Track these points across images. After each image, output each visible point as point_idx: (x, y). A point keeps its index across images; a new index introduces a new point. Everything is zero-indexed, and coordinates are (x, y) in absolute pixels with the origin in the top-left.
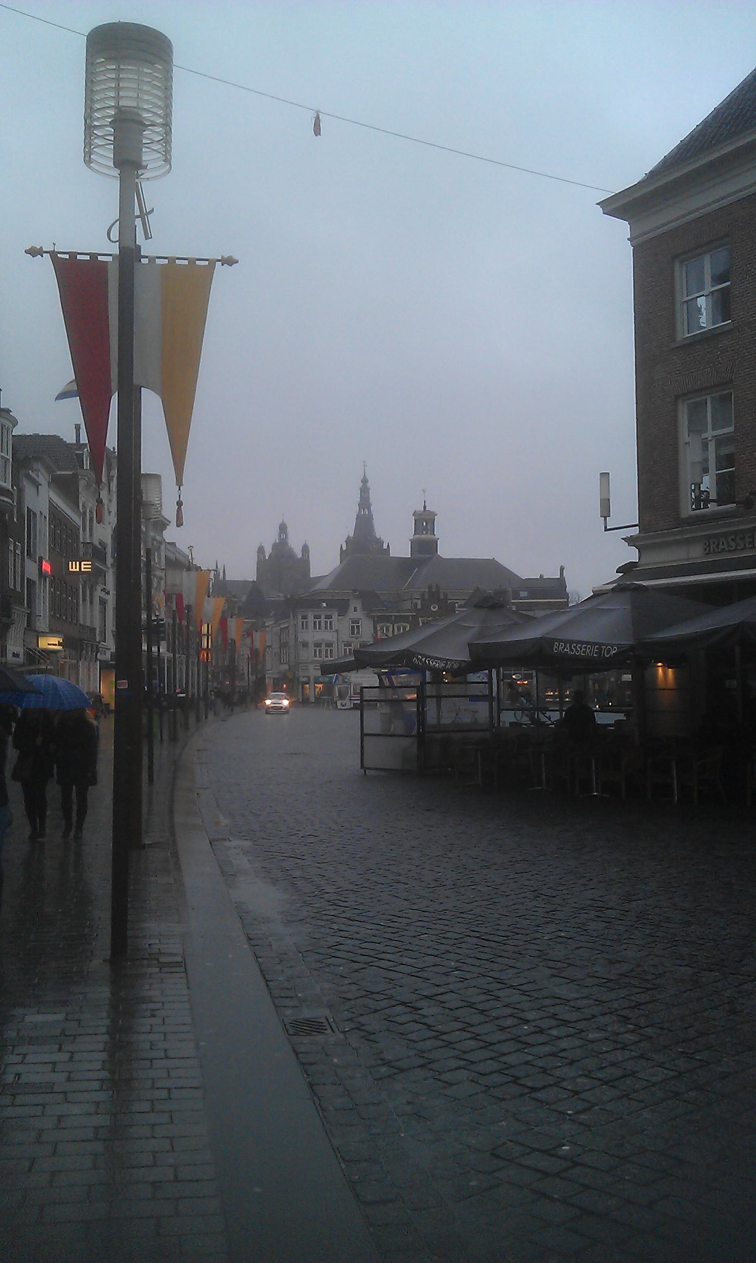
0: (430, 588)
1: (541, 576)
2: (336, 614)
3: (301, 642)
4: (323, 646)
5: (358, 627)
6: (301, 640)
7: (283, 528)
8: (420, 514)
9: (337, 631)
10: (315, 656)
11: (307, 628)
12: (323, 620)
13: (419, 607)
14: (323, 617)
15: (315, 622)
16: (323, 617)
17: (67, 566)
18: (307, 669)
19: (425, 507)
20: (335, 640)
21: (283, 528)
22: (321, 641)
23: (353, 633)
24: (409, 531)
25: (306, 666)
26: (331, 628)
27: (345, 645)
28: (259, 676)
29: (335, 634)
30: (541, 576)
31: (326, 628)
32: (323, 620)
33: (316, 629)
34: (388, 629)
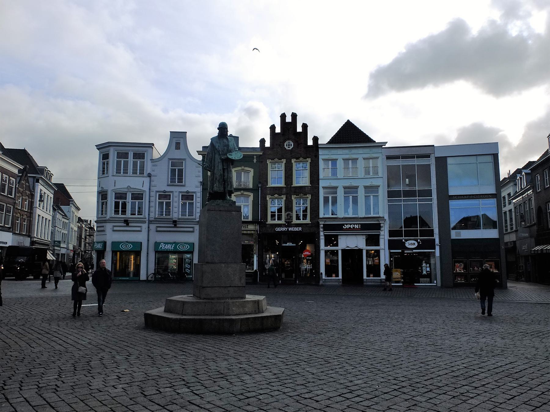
4: (129, 196)
5: (181, 172)
9: (149, 175)
10: (117, 212)
12: (131, 159)
14: (131, 155)
15: (119, 163)
16: (131, 155)
18: (103, 231)
20: (146, 188)
22: (126, 190)
23: (173, 180)
25: (103, 226)
26: (142, 173)
27: (160, 197)
29: (147, 180)
31: (135, 172)
32: (131, 159)
33: (120, 173)
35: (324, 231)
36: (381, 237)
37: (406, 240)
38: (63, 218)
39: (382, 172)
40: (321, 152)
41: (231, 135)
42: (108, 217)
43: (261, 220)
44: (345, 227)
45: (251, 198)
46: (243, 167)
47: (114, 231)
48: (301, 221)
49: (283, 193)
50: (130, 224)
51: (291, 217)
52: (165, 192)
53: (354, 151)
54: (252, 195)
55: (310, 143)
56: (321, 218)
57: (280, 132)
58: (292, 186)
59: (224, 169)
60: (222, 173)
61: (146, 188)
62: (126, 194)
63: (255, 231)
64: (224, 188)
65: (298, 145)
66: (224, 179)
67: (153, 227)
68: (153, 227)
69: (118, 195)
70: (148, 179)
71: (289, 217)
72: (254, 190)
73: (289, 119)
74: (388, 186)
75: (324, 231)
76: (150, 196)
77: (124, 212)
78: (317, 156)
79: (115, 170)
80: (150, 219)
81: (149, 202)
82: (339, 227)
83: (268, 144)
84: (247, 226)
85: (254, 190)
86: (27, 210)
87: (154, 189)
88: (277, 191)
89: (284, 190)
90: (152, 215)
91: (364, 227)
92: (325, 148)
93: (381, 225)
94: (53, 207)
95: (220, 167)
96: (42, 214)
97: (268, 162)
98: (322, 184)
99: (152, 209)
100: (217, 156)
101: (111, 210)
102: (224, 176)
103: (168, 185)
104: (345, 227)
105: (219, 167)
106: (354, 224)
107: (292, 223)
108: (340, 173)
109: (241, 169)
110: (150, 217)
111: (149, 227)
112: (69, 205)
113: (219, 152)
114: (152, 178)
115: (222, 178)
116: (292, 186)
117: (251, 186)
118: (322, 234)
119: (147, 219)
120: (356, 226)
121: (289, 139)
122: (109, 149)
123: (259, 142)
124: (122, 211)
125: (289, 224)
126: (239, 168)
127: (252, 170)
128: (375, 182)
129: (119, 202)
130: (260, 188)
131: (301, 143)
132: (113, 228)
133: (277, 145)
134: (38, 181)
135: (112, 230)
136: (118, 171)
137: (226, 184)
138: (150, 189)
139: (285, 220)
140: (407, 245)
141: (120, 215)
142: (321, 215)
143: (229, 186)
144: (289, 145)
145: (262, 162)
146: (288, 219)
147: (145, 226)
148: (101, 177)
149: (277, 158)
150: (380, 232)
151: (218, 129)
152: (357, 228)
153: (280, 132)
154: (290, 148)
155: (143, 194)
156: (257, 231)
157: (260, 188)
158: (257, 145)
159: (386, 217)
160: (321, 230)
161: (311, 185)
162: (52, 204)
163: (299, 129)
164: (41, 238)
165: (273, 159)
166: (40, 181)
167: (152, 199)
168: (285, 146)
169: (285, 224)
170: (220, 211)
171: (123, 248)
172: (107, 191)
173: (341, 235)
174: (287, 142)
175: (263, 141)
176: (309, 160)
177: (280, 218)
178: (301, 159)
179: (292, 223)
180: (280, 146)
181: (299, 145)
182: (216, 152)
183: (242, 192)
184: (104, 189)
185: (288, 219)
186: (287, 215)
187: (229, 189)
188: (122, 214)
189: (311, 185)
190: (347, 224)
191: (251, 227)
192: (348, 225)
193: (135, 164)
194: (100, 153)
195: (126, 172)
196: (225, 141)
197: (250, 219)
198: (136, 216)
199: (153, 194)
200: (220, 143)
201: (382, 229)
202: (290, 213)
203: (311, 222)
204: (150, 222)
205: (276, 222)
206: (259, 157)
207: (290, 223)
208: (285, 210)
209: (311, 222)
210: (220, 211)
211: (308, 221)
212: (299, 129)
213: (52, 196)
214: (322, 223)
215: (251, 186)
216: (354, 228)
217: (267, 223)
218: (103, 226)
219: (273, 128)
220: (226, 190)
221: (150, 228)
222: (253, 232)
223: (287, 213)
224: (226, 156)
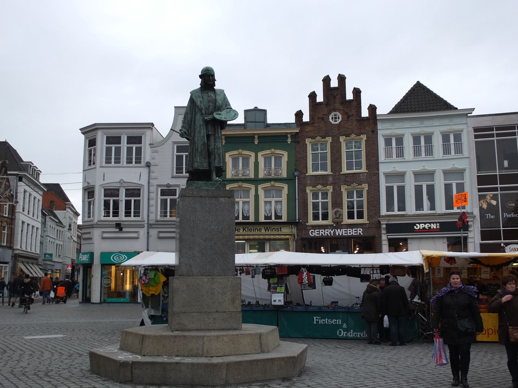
0: (327, 80)
4: (122, 193)
10: (107, 214)
12: (124, 145)
15: (109, 150)
18: (90, 239)
20: (144, 181)
22: (118, 185)
25: (89, 233)
26: (138, 161)
27: (163, 193)
29: (145, 171)
31: (129, 161)
32: (124, 145)
33: (110, 163)
34: (246, 159)
35: (387, 233)
36: (469, 240)
37: (507, 244)
38: (57, 225)
40: (380, 126)
41: (256, 107)
42: (96, 221)
43: (299, 220)
44: (417, 227)
45: (285, 192)
46: (273, 150)
47: (103, 238)
48: (356, 221)
49: (329, 183)
50: (124, 230)
51: (341, 215)
52: (168, 185)
53: (427, 123)
54: (286, 187)
55: (365, 113)
56: (383, 216)
57: (322, 101)
58: (341, 173)
59: (208, 136)
60: (206, 141)
61: (144, 181)
62: (118, 190)
63: (291, 235)
64: (210, 164)
65: (348, 117)
66: (208, 149)
67: (154, 232)
68: (154, 232)
69: (109, 192)
70: (146, 170)
71: (338, 216)
73: (334, 83)
74: (479, 169)
75: (387, 233)
76: (149, 192)
77: (116, 213)
78: (374, 132)
79: (104, 160)
80: (150, 222)
81: (149, 199)
82: (409, 228)
83: (306, 118)
84: (281, 228)
86: (7, 216)
87: (154, 182)
88: (322, 180)
89: (331, 179)
90: (152, 217)
91: (445, 227)
92: (386, 120)
93: (469, 223)
94: (42, 212)
95: (203, 132)
96: (27, 220)
97: (308, 141)
98: (383, 169)
99: (152, 209)
100: (198, 117)
101: (100, 211)
102: (209, 146)
103: (173, 177)
104: (417, 227)
105: (201, 132)
106: (430, 223)
107: (342, 223)
109: (270, 152)
110: (150, 219)
111: (148, 233)
112: (65, 210)
113: (201, 110)
114: (152, 168)
115: (206, 149)
116: (341, 173)
117: (284, 175)
118: (384, 237)
119: (146, 222)
120: (433, 226)
121: (335, 110)
122: (97, 133)
123: (294, 116)
124: (113, 213)
125: (338, 225)
126: (268, 152)
127: (286, 154)
128: (459, 165)
129: (109, 200)
130: (297, 178)
131: (353, 115)
132: (102, 235)
133: (318, 118)
134: (20, 179)
135: (100, 237)
136: (108, 161)
137: (213, 157)
138: (149, 183)
139: (333, 219)
141: (111, 218)
142: (384, 211)
143: (217, 161)
144: (336, 118)
145: (298, 142)
146: (337, 218)
147: (143, 232)
148: (87, 168)
149: (320, 136)
150: (467, 233)
151: (201, 77)
152: (435, 228)
153: (322, 101)
154: (338, 122)
155: (139, 190)
156: (294, 235)
157: (297, 178)
158: (292, 120)
160: (384, 232)
161: (367, 171)
162: (41, 208)
163: (349, 96)
164: (26, 250)
165: (313, 138)
166: (24, 180)
167: (153, 195)
168: (331, 120)
169: (333, 225)
170: (201, 197)
172: (93, 187)
173: (412, 238)
174: (333, 114)
175: (299, 115)
176: (364, 137)
177: (325, 217)
178: (353, 136)
179: (342, 223)
180: (323, 120)
181: (350, 118)
182: (197, 111)
183: (273, 183)
184: (91, 184)
185: (337, 218)
186: (336, 213)
187: (216, 165)
188: (113, 216)
189: (367, 171)
190: (419, 223)
191: (286, 230)
192: (421, 225)
193: (129, 150)
194: (86, 138)
195: (118, 160)
196: (211, 94)
197: (284, 219)
198: (132, 218)
199: (152, 189)
200: (203, 97)
201: (470, 229)
202: (339, 210)
203: (368, 222)
204: (150, 226)
205: (320, 222)
206: (294, 136)
207: (339, 224)
208: (332, 207)
209: (368, 222)
210: (201, 197)
212: (349, 96)
213: (41, 198)
214: (384, 223)
215: (284, 175)
216: (430, 228)
217: (307, 224)
218: (89, 233)
219: (313, 96)
220: (212, 166)
221: (150, 233)
222: (288, 236)
223: (335, 210)
224: (211, 117)
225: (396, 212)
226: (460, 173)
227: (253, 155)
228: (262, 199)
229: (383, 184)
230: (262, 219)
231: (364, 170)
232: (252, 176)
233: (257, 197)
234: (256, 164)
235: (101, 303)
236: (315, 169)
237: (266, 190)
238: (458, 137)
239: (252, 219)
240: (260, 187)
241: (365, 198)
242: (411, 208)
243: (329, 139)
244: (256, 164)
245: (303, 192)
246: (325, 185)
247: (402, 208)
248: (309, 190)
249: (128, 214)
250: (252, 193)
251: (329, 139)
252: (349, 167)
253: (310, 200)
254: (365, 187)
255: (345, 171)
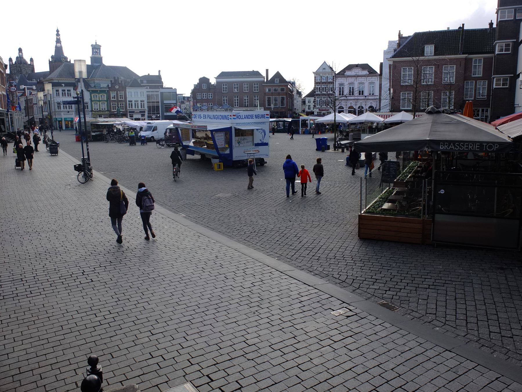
1: (149, 74)
2: (72, 89)
3: (56, 102)
6: (57, 101)
7: (20, 50)
8: (94, 46)
10: (64, 109)
11: (59, 96)
13: (110, 86)
15: (63, 93)
17: (397, 56)
19: (96, 43)
21: (20, 50)
24: (90, 54)
28: (30, 117)
30: (149, 74)
31: (68, 96)
32: (66, 92)
34: (96, 96)
39: (145, 96)
42: (62, 111)
54: (106, 102)
72: (107, 101)
73: (116, 78)
74: (148, 100)
77: (66, 109)
78: (126, 91)
82: (133, 112)
85: (107, 101)
89: (116, 101)
91: (141, 112)
97: (111, 92)
98: (128, 99)
108: (133, 96)
117: (106, 100)
118: (128, 114)
121: (116, 85)
127: (106, 95)
128: (143, 99)
136: (63, 96)
140: (153, 117)
141: (65, 110)
142: (128, 108)
154: (118, 88)
159: (147, 109)
171: (68, 119)
176: (123, 92)
191: (107, 112)
193: (68, 93)
195: (65, 96)
197: (106, 110)
205: (114, 110)
211: (124, 110)
212: (120, 82)
214: (128, 111)
215: (106, 100)
225: (131, 109)
226: (143, 101)
227: (98, 95)
228: (101, 105)
229: (128, 103)
230: (101, 110)
231: (123, 99)
232: (98, 100)
233: (100, 105)
234: (99, 97)
235: (65, 130)
236: (113, 98)
237: (102, 103)
238: (143, 93)
239: (99, 110)
240: (100, 102)
241: (124, 105)
242: (134, 108)
243: (116, 92)
244: (99, 97)
245: (110, 104)
246: (115, 102)
247: (132, 108)
248: (112, 103)
249: (69, 109)
250: (98, 104)
251: (116, 92)
252: (120, 98)
253: (112, 106)
254: (124, 103)
255: (119, 99)
